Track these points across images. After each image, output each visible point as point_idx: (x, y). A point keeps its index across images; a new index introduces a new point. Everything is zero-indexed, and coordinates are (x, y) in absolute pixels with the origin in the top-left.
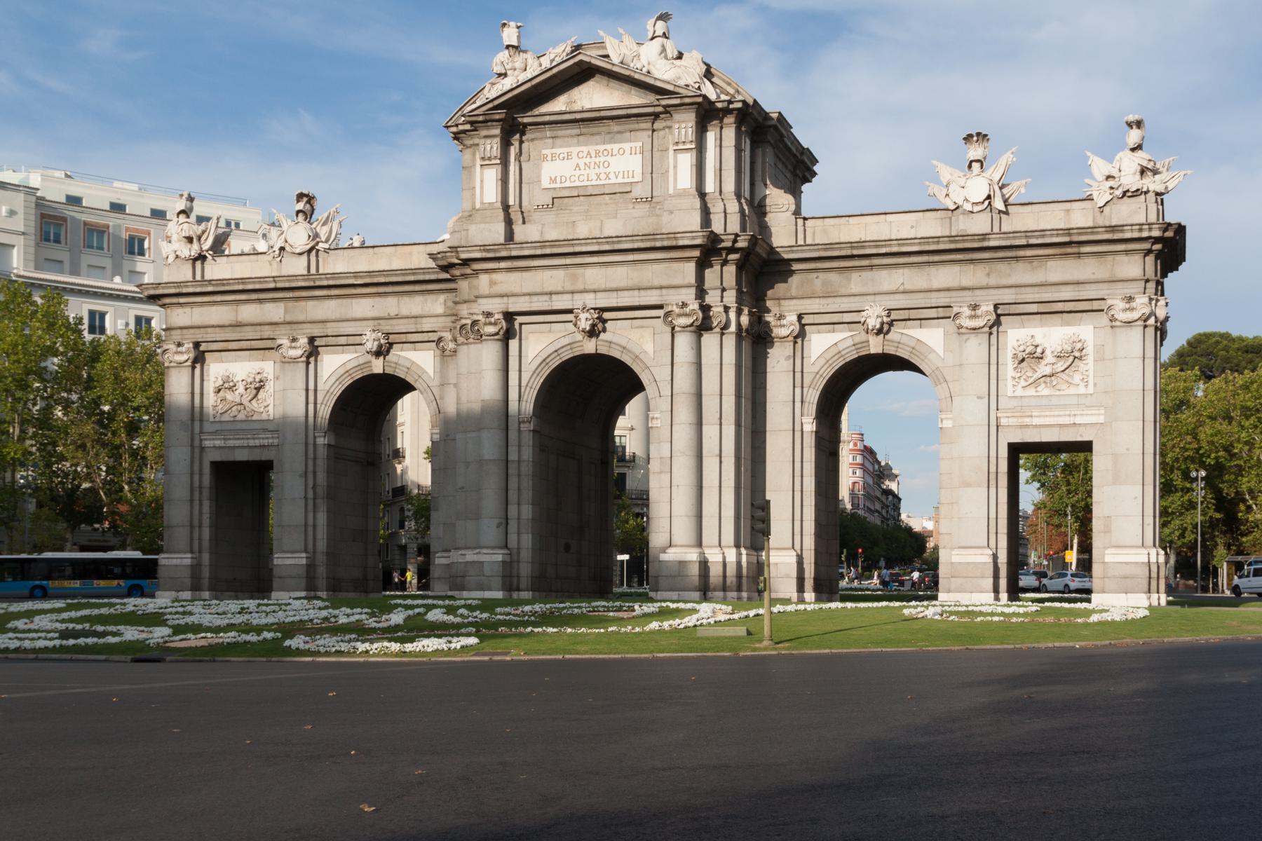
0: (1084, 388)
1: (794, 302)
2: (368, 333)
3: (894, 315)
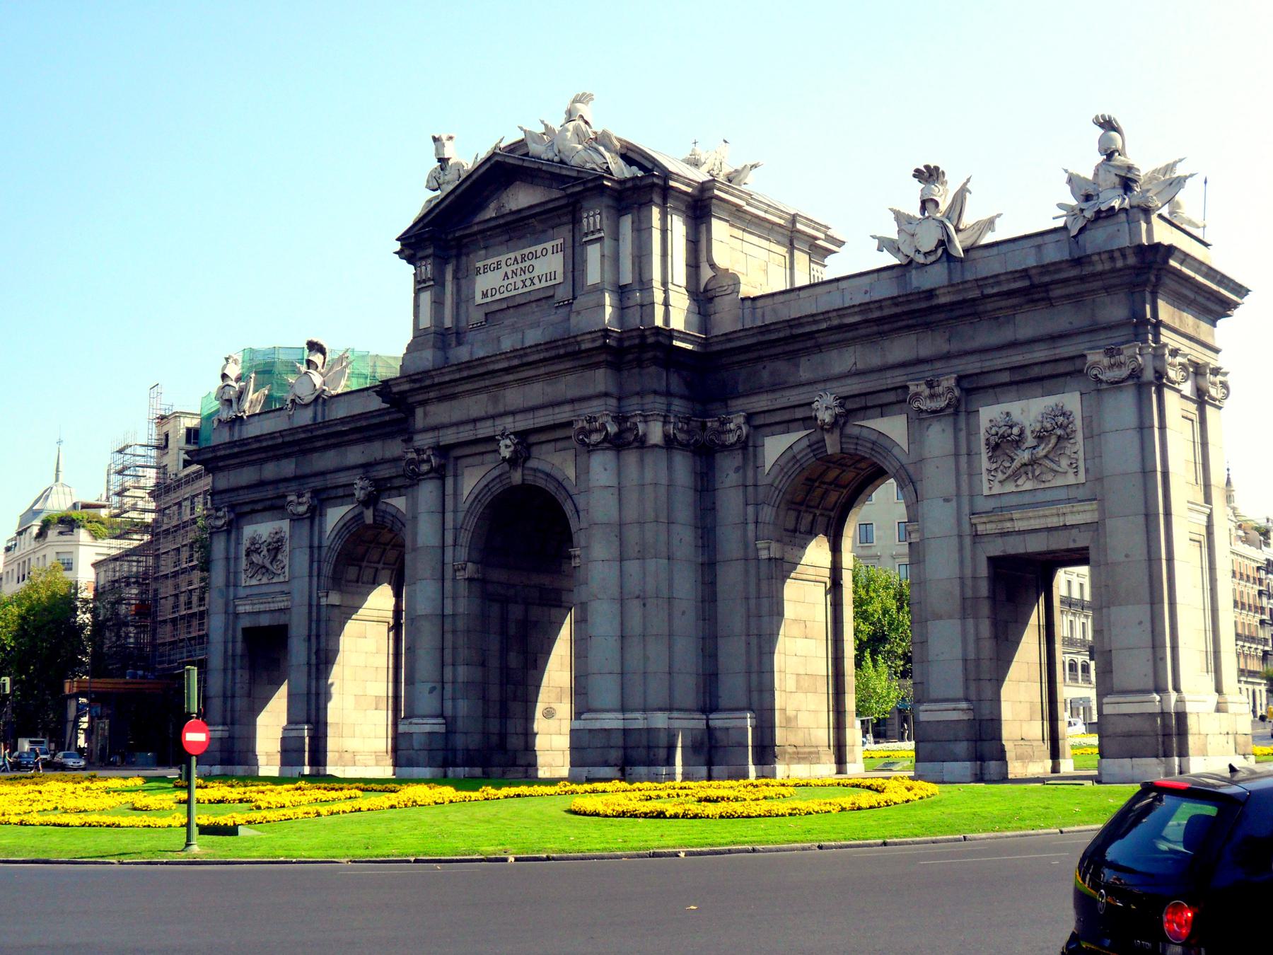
0: (1073, 475)
1: (740, 401)
2: (357, 481)
3: (850, 405)
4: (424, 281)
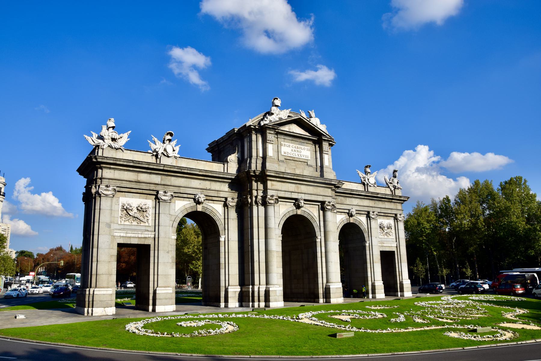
4: (270, 141)
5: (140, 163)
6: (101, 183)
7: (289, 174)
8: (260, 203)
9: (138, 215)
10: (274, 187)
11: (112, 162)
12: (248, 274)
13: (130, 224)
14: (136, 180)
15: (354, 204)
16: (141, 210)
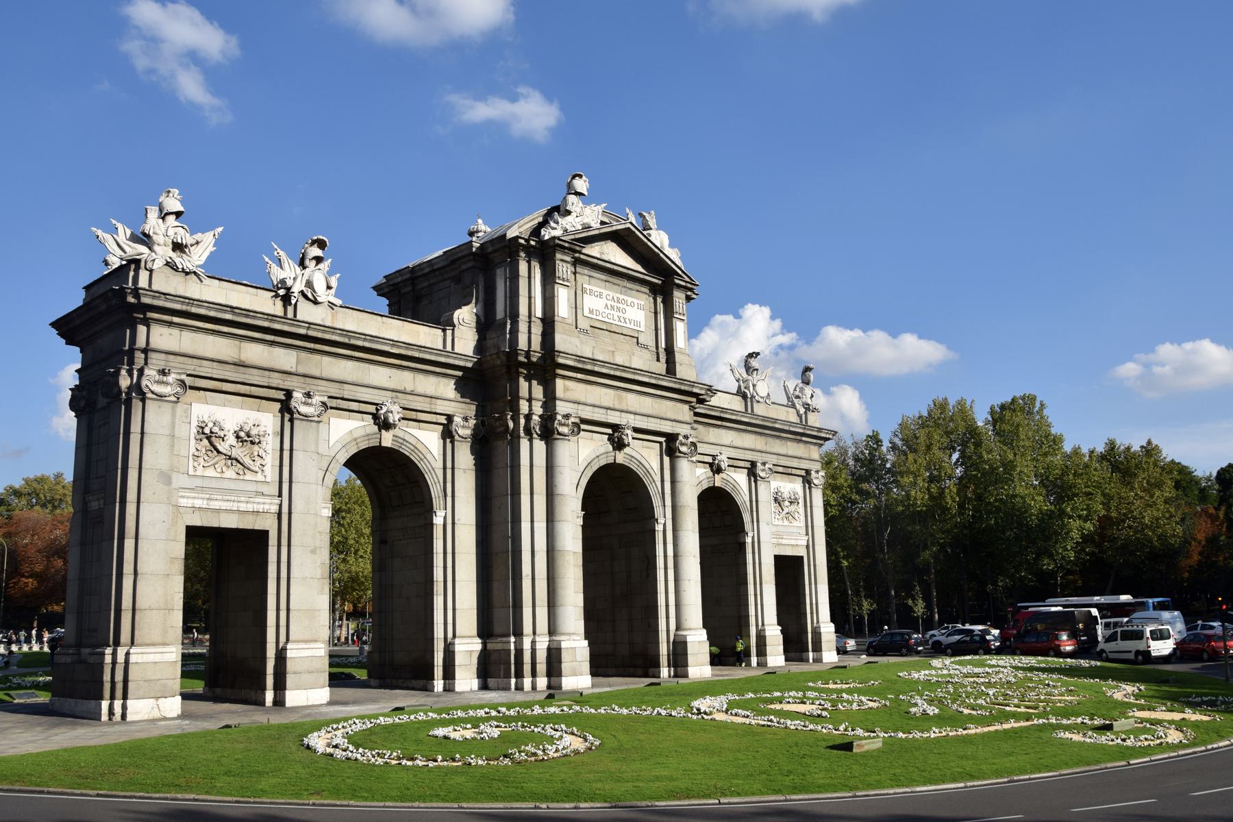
4: (563, 280)
5: (251, 314)
6: (146, 363)
7: (606, 365)
8: (537, 434)
9: (238, 452)
10: (569, 395)
11: (178, 307)
12: (503, 607)
13: (219, 475)
14: (236, 360)
15: (723, 442)
16: (246, 438)
